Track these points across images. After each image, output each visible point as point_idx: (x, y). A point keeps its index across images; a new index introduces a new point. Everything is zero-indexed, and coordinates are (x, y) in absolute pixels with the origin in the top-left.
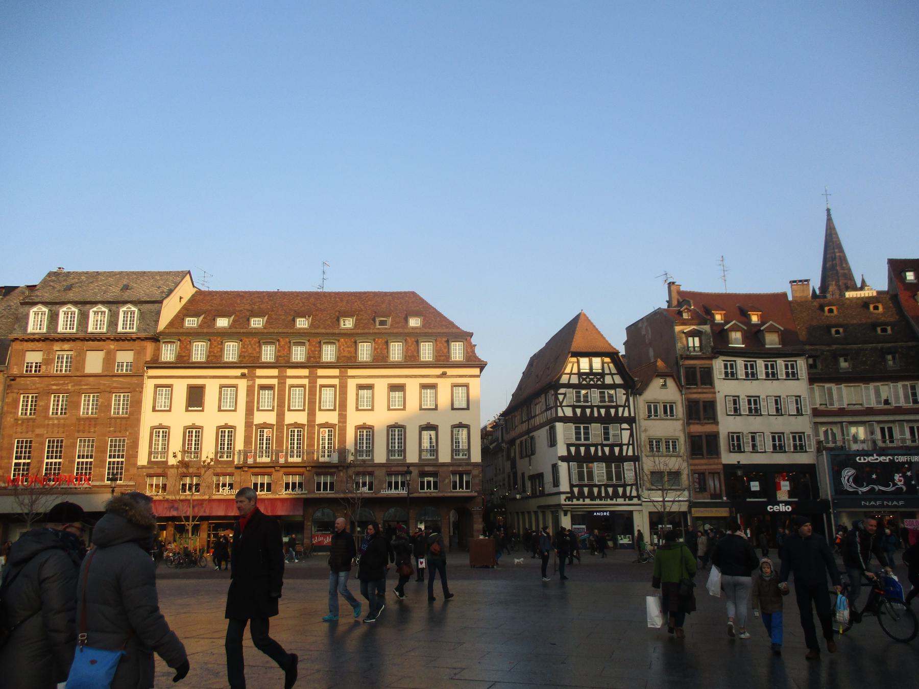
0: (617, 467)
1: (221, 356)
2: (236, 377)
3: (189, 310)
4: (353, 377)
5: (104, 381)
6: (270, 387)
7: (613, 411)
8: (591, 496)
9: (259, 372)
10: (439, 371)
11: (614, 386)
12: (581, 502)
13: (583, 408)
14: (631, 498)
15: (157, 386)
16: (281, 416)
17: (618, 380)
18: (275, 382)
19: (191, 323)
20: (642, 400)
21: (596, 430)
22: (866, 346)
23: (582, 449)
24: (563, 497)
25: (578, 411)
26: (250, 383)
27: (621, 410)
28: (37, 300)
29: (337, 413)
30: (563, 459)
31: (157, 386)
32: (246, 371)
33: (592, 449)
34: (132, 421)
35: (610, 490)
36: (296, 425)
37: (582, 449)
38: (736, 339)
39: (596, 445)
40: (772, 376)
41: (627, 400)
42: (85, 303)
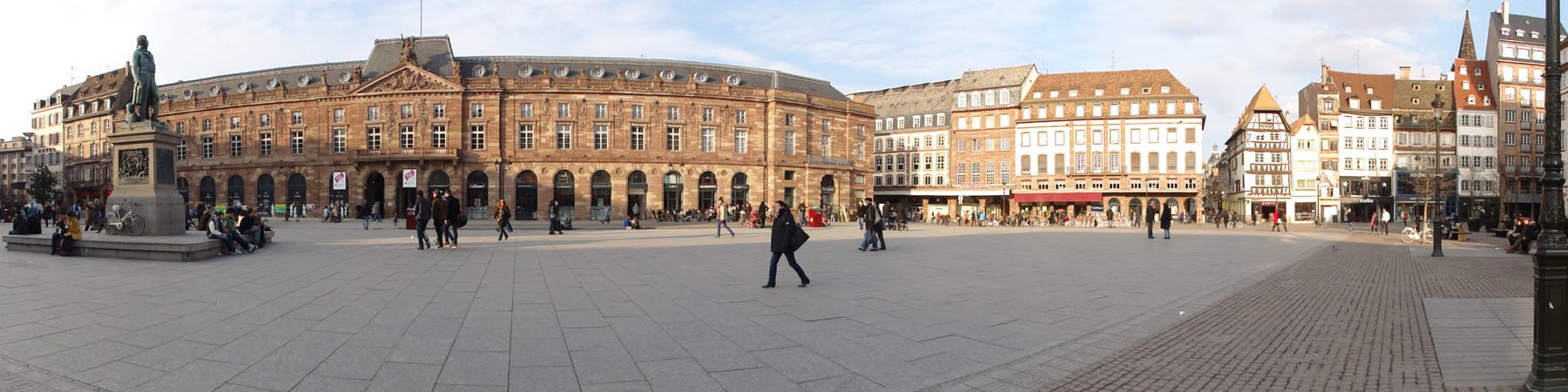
1: (1054, 115)
3: (1035, 89)
5: (996, 131)
7: (1278, 145)
8: (1263, 193)
9: (1075, 123)
12: (1256, 196)
14: (1285, 195)
16: (1089, 147)
19: (1037, 95)
21: (1268, 157)
23: (1259, 167)
25: (1258, 145)
27: (1282, 144)
28: (961, 89)
29: (1120, 144)
30: (1248, 172)
32: (1068, 122)
34: (1010, 153)
35: (1274, 190)
36: (1098, 153)
37: (1259, 167)
42: (983, 89)
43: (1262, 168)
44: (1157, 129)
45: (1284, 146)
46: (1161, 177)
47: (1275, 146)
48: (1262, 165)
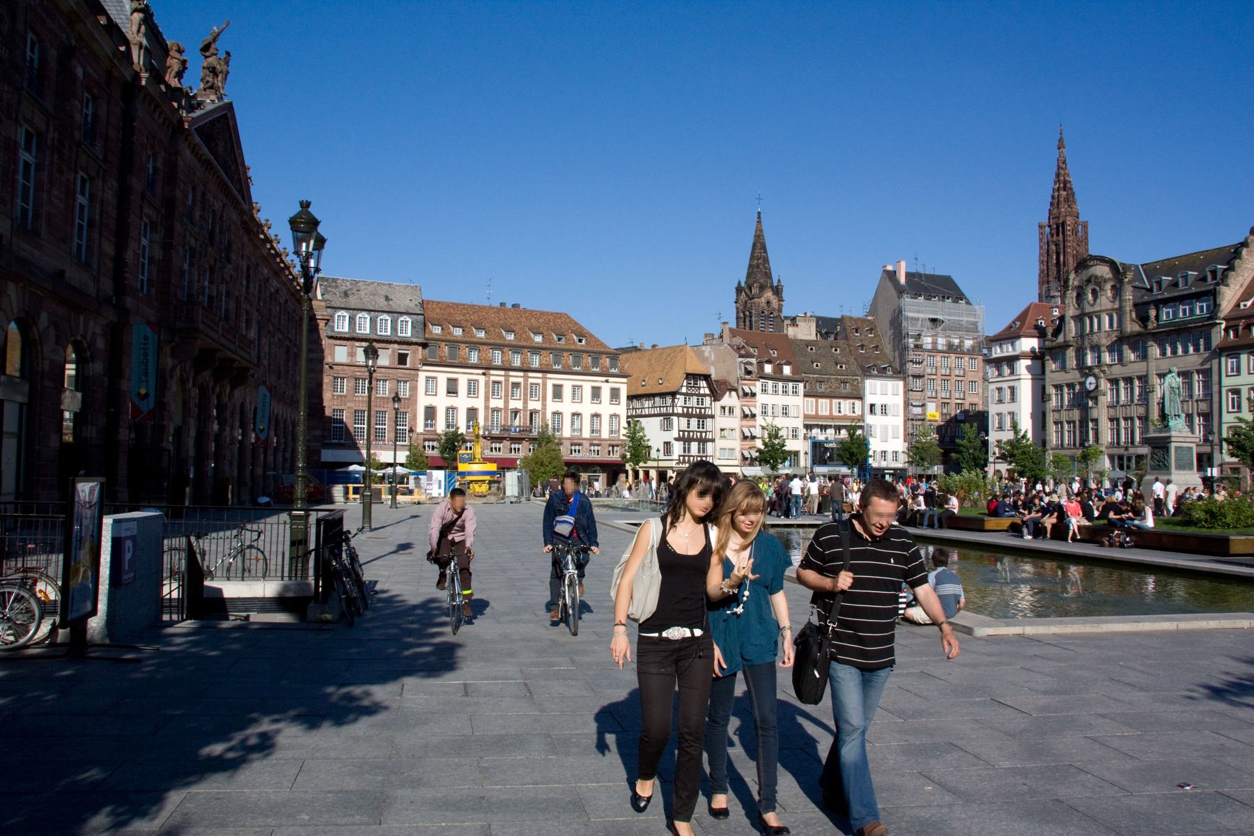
0: (703, 445)
2: (478, 374)
4: (551, 378)
6: (499, 382)
7: (703, 410)
9: (492, 372)
10: (604, 379)
11: (705, 395)
13: (688, 408)
15: (427, 377)
16: (506, 402)
17: (707, 391)
18: (502, 379)
20: (718, 404)
22: (832, 377)
23: (686, 433)
24: (675, 462)
25: (685, 410)
26: (487, 379)
29: (540, 402)
30: (676, 439)
31: (427, 377)
32: (484, 371)
33: (691, 434)
34: (413, 399)
37: (686, 433)
38: (768, 369)
39: (693, 432)
40: (785, 392)
41: (711, 404)
43: (689, 435)
44: (581, 386)
45: (709, 412)
46: (584, 442)
47: (700, 412)
48: (689, 432)
